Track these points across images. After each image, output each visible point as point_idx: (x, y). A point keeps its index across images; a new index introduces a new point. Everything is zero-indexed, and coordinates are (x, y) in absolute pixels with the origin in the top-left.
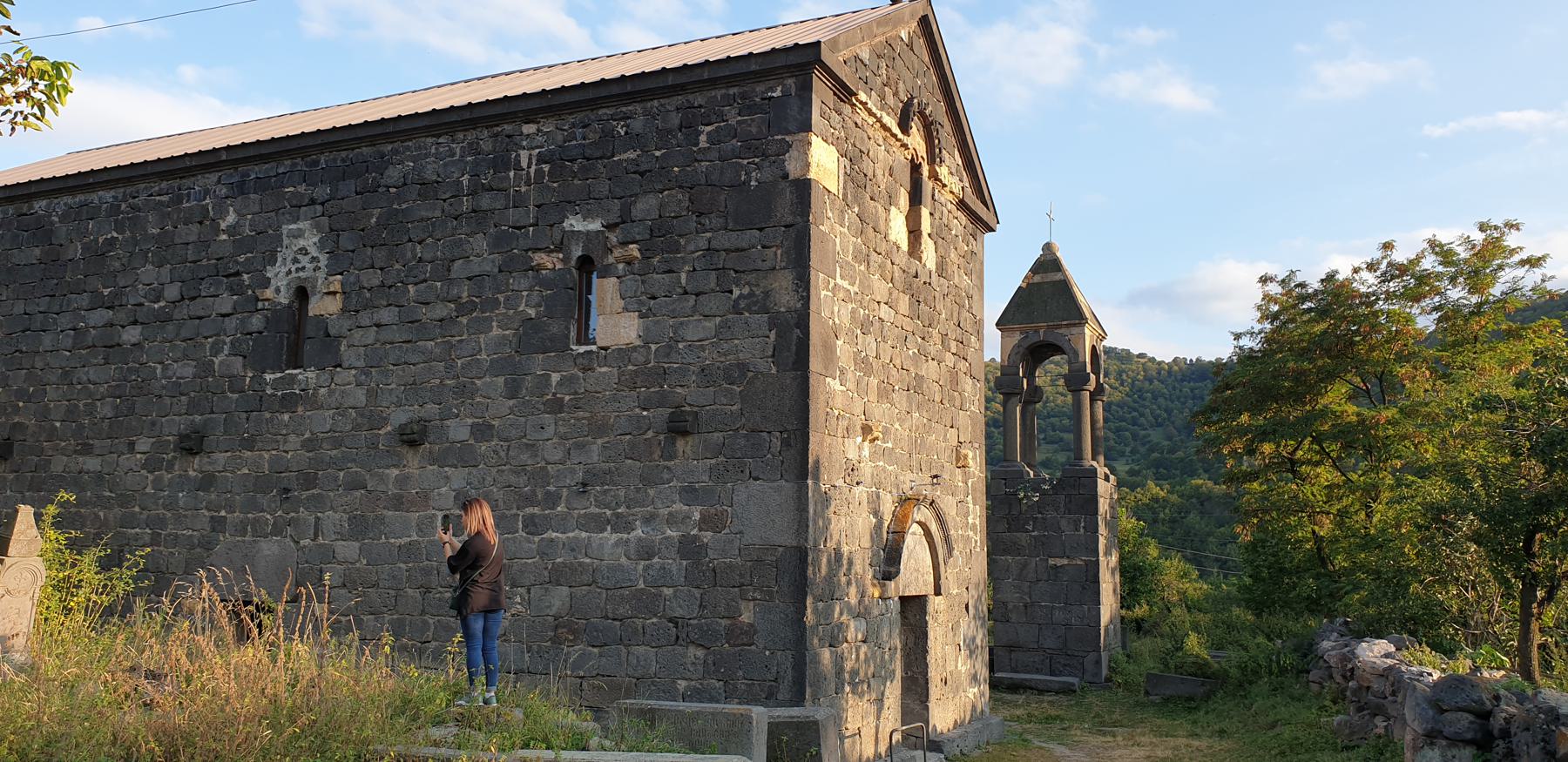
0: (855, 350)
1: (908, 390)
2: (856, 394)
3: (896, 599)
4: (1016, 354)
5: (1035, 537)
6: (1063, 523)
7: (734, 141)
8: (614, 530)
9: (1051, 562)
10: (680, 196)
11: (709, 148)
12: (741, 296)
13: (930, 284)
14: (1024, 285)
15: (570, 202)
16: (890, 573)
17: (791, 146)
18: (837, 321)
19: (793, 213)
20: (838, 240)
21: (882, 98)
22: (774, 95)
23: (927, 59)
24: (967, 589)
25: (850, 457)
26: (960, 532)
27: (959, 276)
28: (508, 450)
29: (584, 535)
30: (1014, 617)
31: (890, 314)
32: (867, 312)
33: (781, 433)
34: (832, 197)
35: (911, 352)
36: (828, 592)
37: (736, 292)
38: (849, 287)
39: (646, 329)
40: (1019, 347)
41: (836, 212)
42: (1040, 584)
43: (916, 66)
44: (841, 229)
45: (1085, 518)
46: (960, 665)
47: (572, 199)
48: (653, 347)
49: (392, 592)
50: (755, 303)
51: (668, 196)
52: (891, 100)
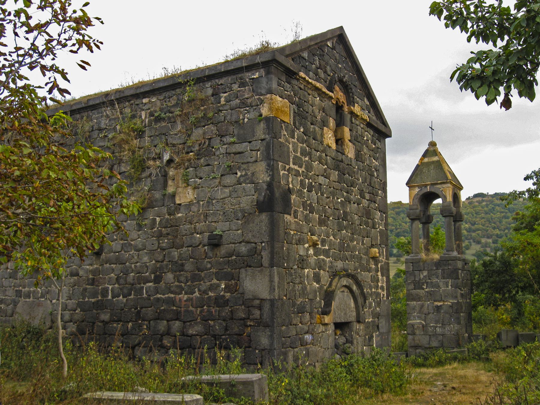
1: (338, 219)
2: (304, 223)
3: (332, 324)
5: (427, 292)
6: (441, 284)
7: (237, 100)
8: (186, 293)
10: (213, 128)
11: (225, 104)
12: (241, 176)
13: (351, 165)
14: (420, 164)
15: (163, 134)
16: (326, 311)
17: (263, 101)
18: (291, 186)
19: (264, 133)
20: (291, 146)
21: (316, 74)
22: (255, 77)
23: (344, 54)
24: (378, 318)
25: (301, 254)
26: (373, 290)
27: (370, 160)
28: (138, 255)
29: (172, 296)
30: (417, 332)
31: (325, 181)
32: (310, 181)
33: (261, 243)
34: (286, 124)
35: (339, 200)
36: (288, 321)
37: (239, 174)
38: (298, 169)
39: (198, 195)
41: (289, 132)
43: (338, 58)
44: (293, 140)
47: (164, 132)
48: (201, 203)
49: (91, 324)
50: (248, 179)
51: (207, 128)
52: (322, 75)
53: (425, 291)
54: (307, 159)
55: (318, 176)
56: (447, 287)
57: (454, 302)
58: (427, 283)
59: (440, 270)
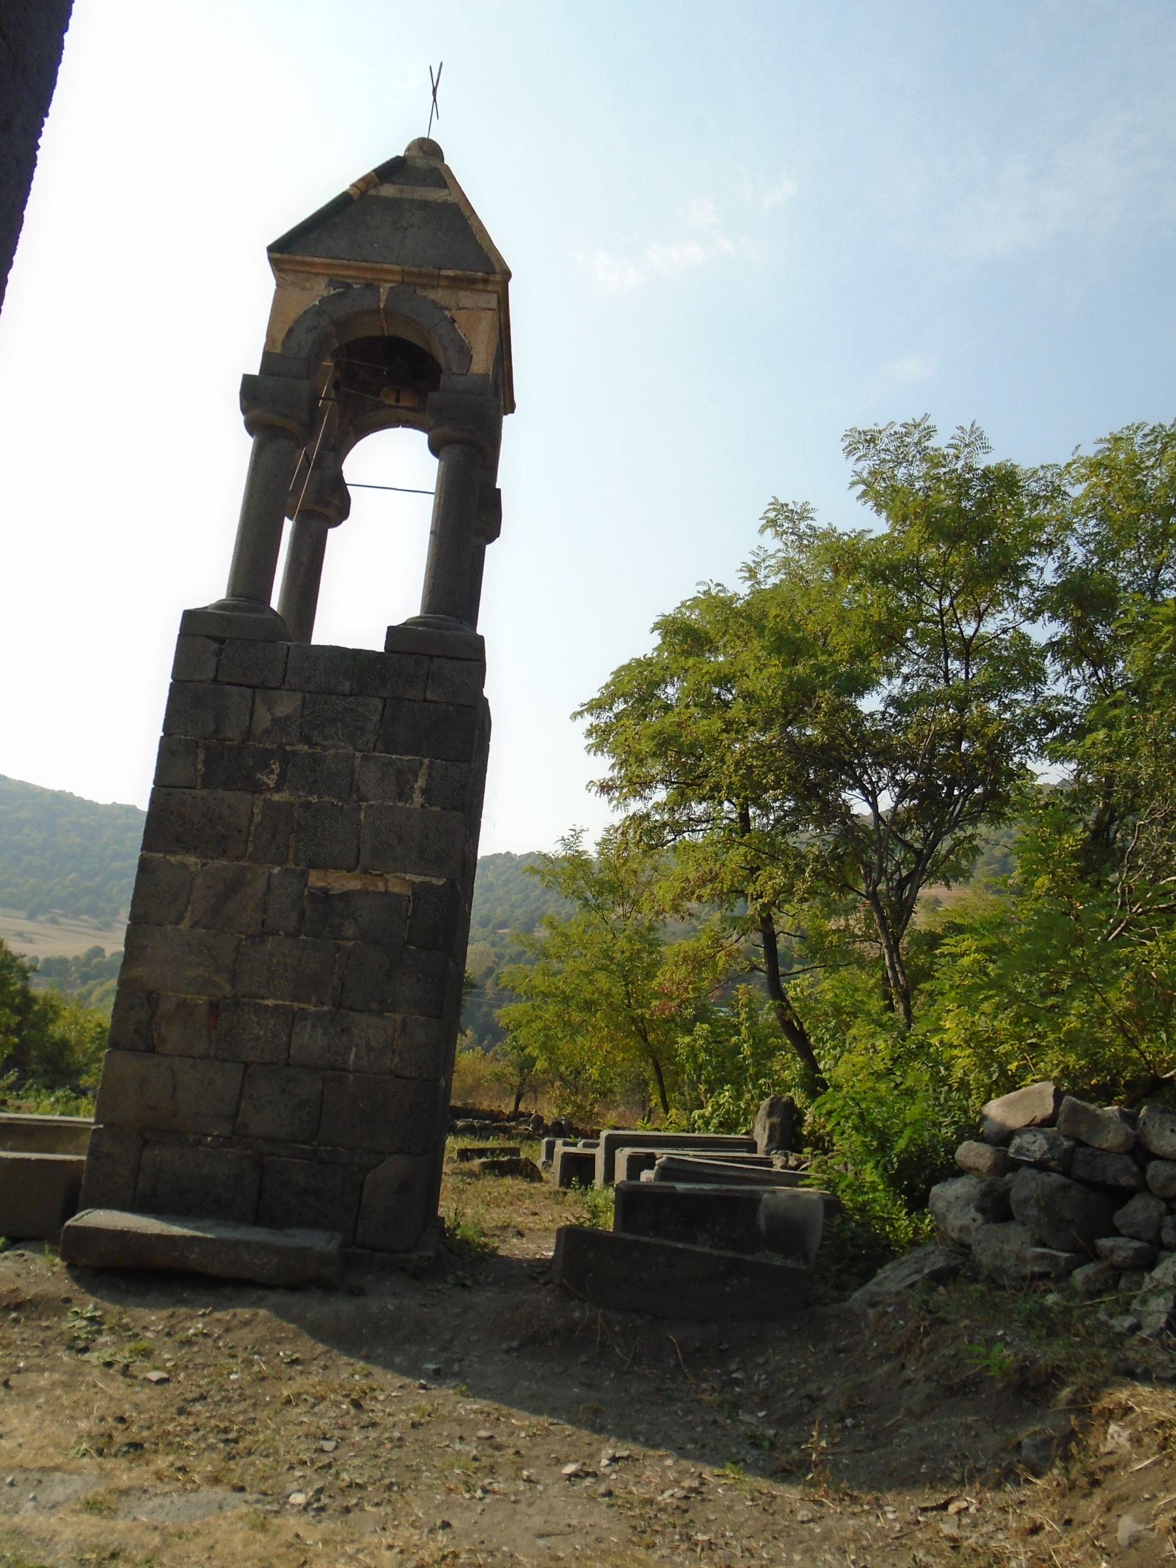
4: (310, 330)
9: (316, 880)
14: (356, 193)
40: (318, 313)
42: (270, 943)
45: (431, 764)
53: (269, 804)
56: (403, 794)
57: (428, 885)
58: (286, 759)
59: (379, 704)
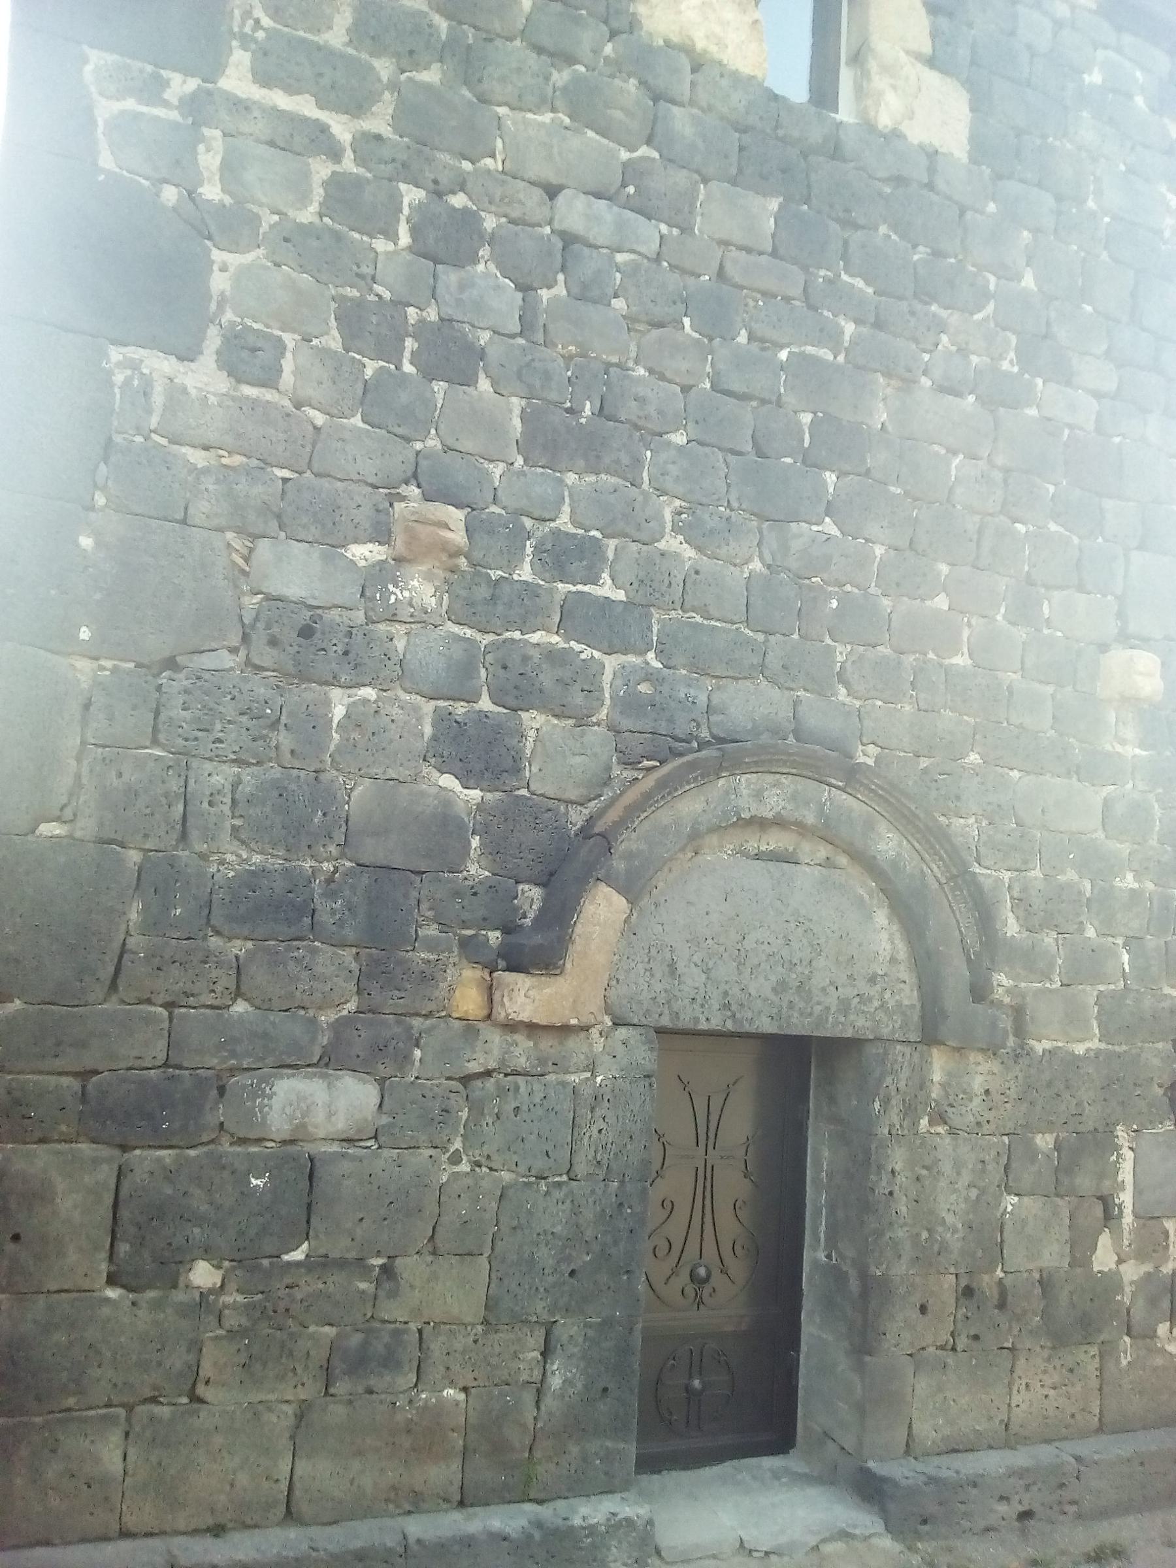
0: (352, 292)
2: (357, 421)
13: (930, 186)
25: (294, 591)
35: (783, 355)
46: (1104, 1258)
54: (431, 76)
55: (552, 192)
